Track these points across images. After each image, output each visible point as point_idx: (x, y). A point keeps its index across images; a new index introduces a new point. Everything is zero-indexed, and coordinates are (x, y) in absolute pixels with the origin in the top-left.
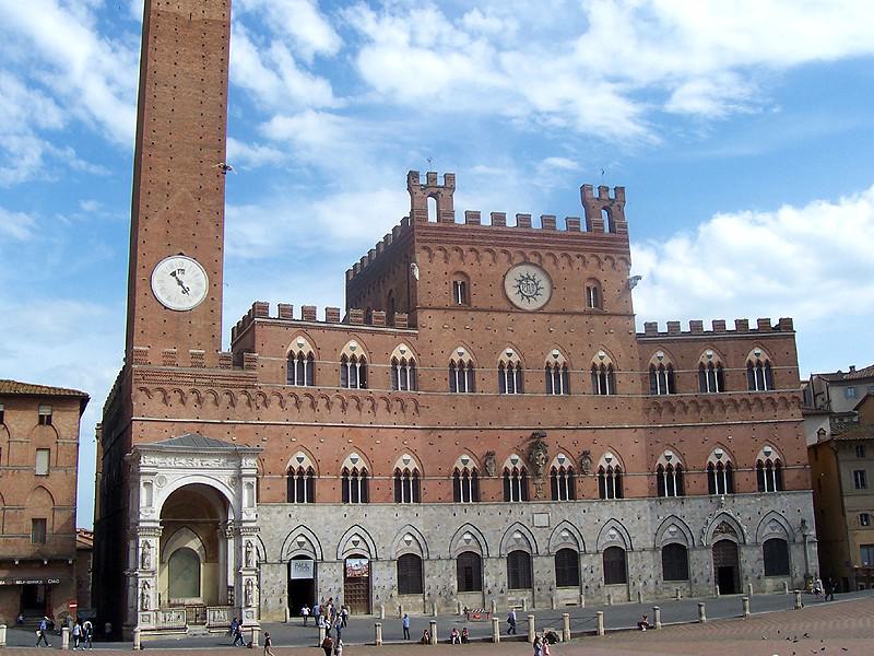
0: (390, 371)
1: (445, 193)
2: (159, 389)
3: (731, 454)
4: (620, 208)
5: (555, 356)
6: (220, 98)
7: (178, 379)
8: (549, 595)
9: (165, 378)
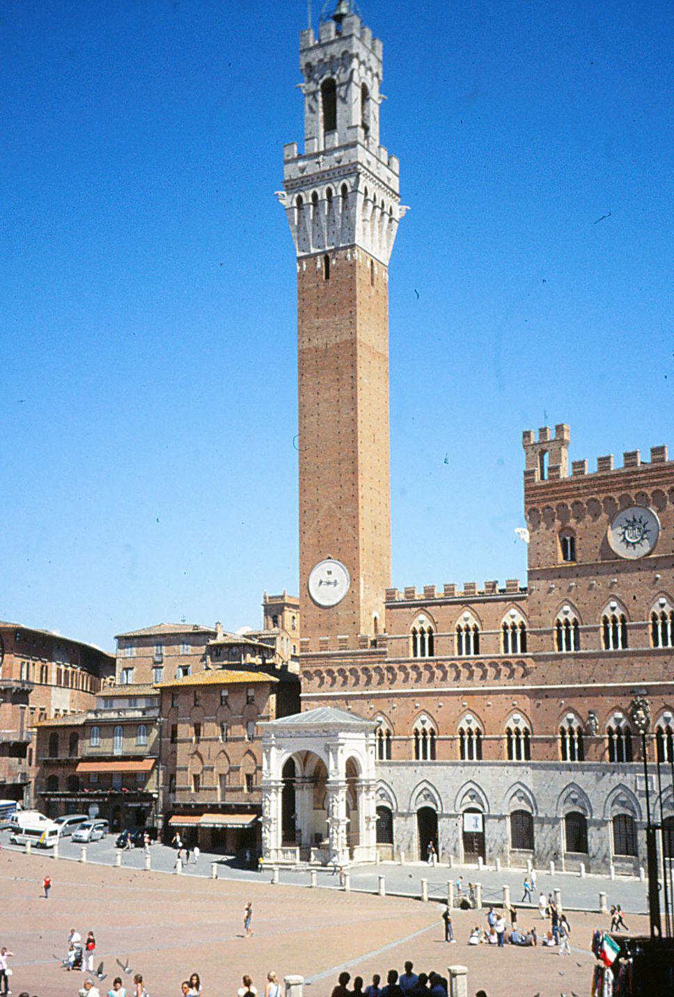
6: (352, 414)
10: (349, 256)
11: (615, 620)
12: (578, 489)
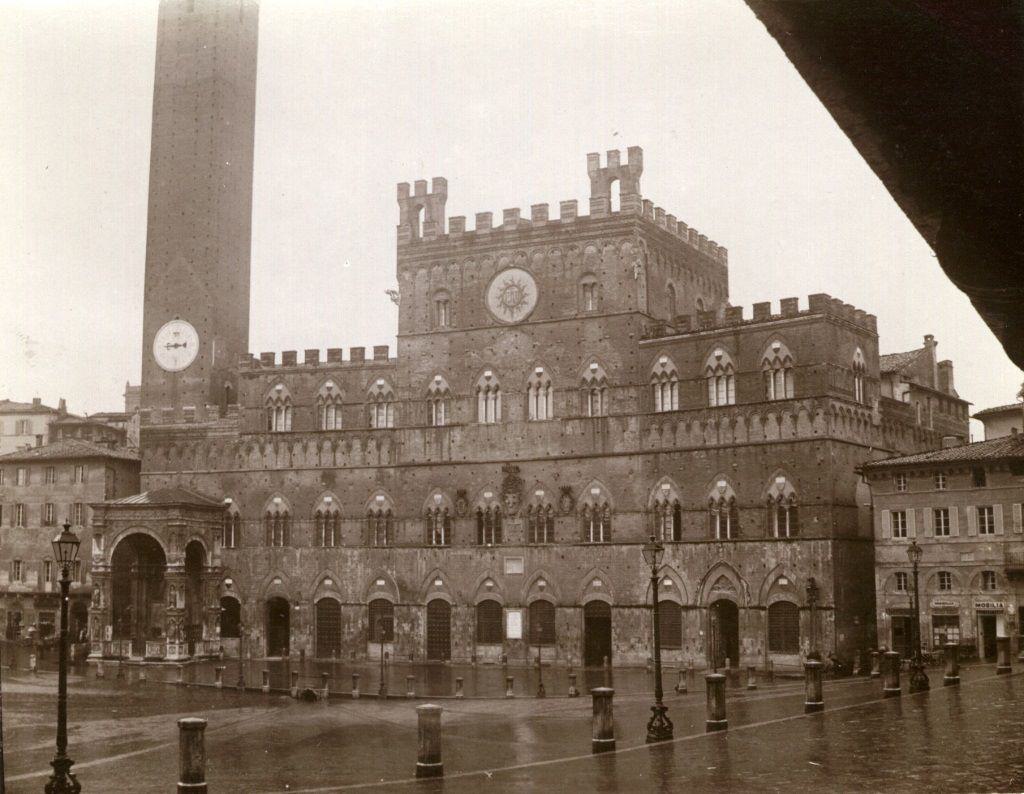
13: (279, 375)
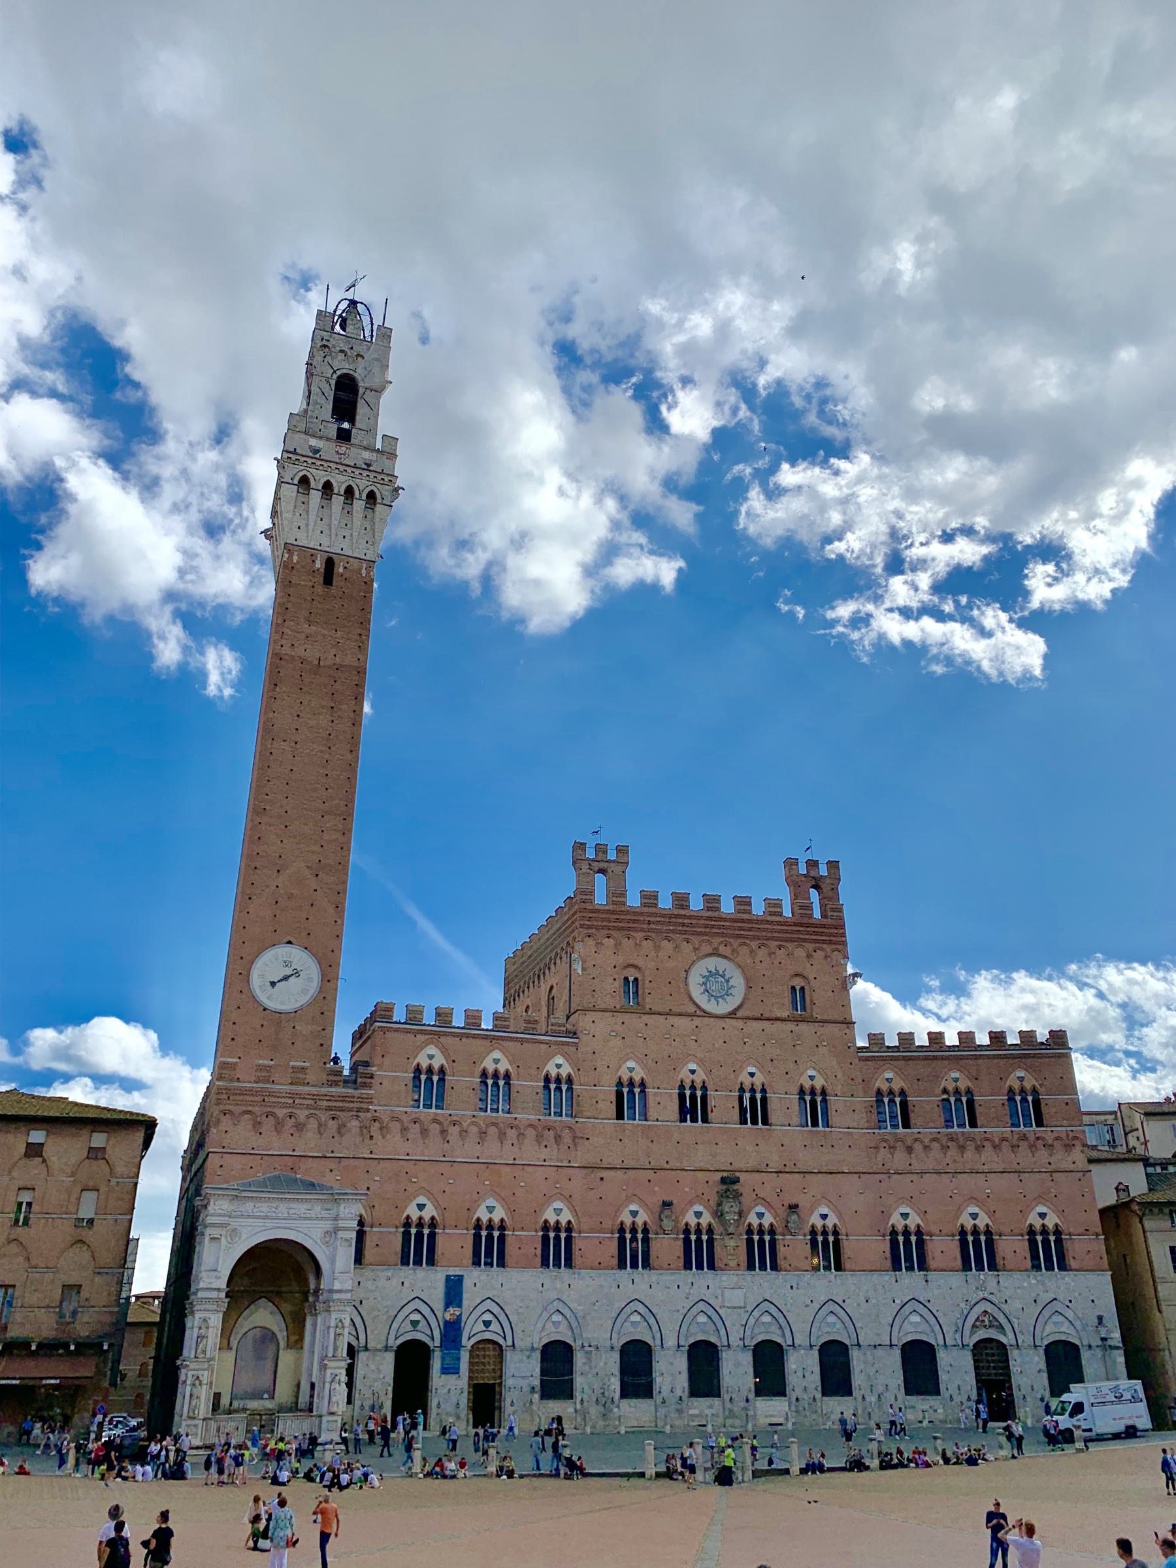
0: (540, 1090)
1: (618, 869)
2: (248, 1112)
3: (992, 1214)
4: (834, 890)
5: (752, 1074)
6: (350, 757)
7: (273, 1099)
8: (745, 1409)
9: (256, 1099)
10: (364, 572)
11: (693, 1088)
12: (649, 923)
13: (434, 1035)
